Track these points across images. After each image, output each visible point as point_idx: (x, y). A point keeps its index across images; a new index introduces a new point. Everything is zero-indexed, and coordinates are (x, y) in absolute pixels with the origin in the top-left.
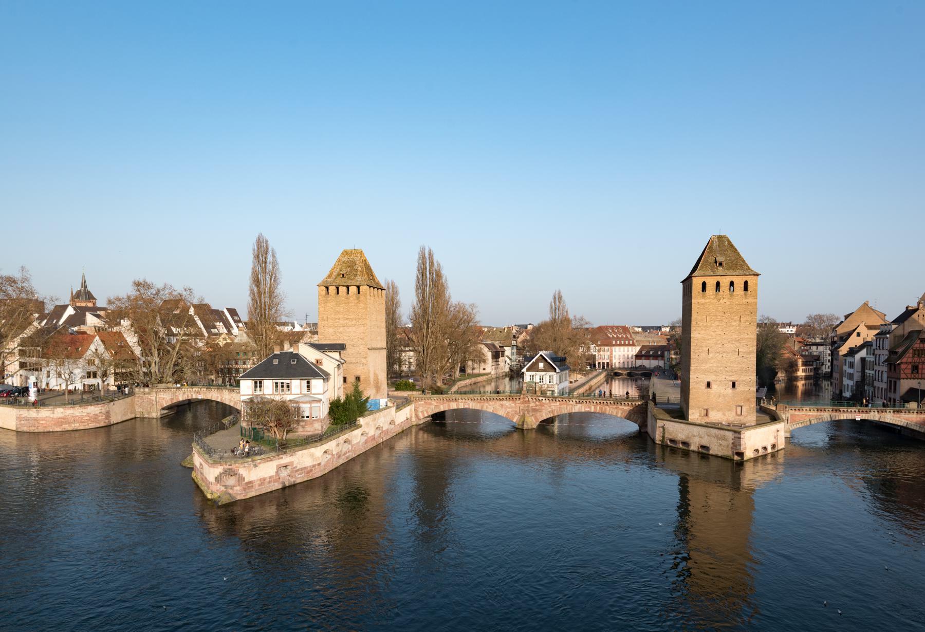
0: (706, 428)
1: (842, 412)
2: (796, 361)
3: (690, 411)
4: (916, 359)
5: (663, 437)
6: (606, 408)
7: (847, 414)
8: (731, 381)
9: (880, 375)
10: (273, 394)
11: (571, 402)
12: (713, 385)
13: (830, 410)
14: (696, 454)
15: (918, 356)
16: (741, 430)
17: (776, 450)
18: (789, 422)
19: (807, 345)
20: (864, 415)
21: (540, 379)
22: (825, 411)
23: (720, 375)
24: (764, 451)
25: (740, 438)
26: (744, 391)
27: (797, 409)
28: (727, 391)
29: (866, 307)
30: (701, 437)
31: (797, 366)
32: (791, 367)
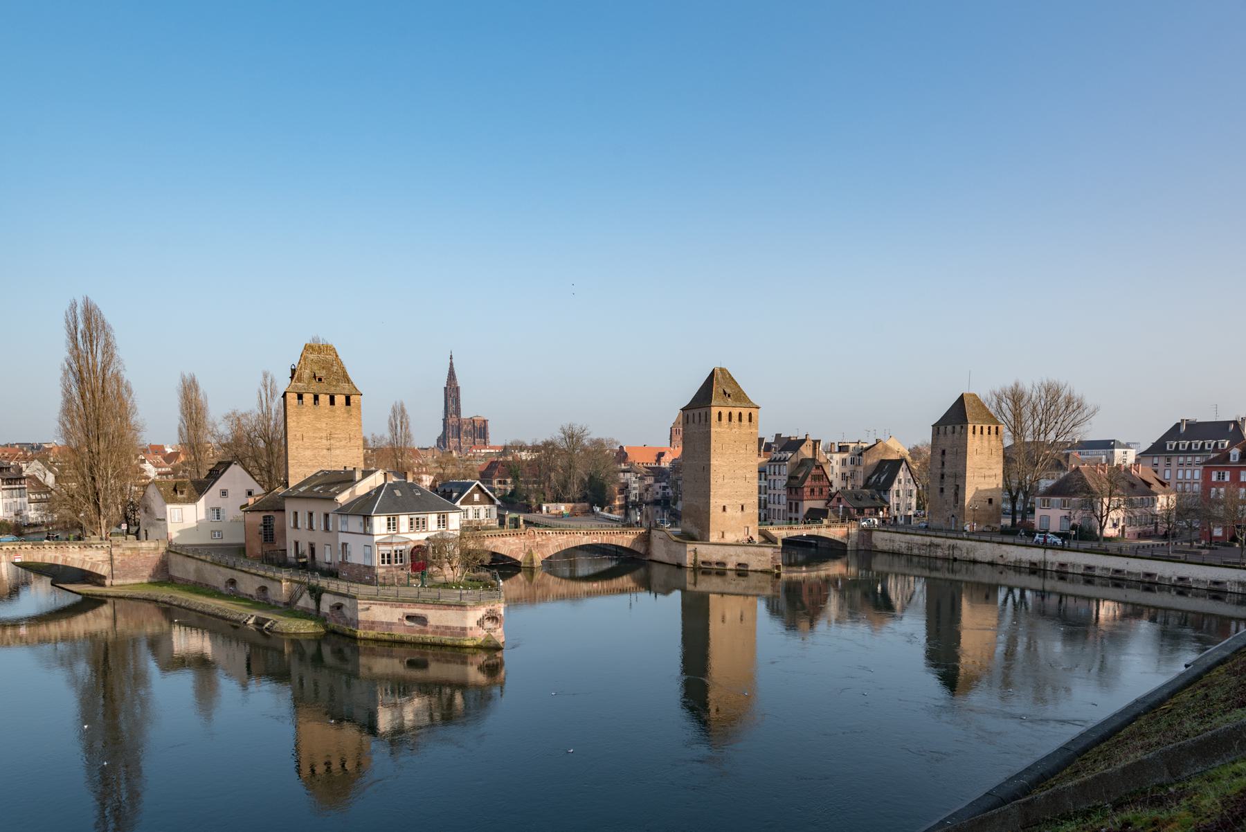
3: (711, 534)
9: (776, 498)
10: (410, 532)
12: (728, 509)
14: (734, 572)
30: (738, 556)
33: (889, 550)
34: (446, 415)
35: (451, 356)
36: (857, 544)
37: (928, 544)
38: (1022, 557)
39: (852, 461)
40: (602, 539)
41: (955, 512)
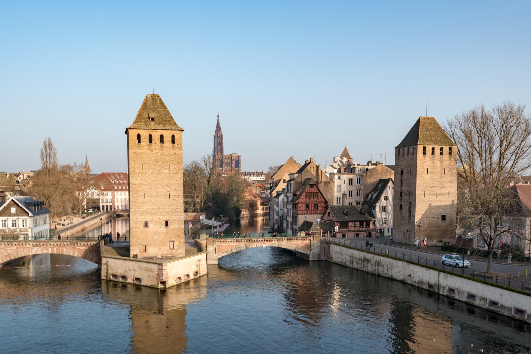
0: (139, 263)
1: (253, 241)
2: (256, 202)
4: (307, 199)
5: (107, 273)
6: (63, 249)
7: (257, 243)
8: (164, 220)
11: (28, 246)
12: (150, 225)
13: (245, 241)
14: (132, 286)
15: (309, 197)
16: (163, 262)
17: (198, 276)
18: (217, 251)
19: (265, 189)
20: (268, 243)
21: (13, 224)
22: (242, 241)
23: (155, 216)
24: (187, 278)
25: (162, 269)
26: (175, 229)
27: (222, 241)
28: (161, 229)
29: (291, 160)
31: (257, 206)
32: (252, 206)
33: (339, 262)
34: (214, 153)
35: (218, 115)
36: (319, 255)
37: (363, 258)
38: (423, 279)
39: (359, 181)
40: (52, 250)
41: (409, 227)
